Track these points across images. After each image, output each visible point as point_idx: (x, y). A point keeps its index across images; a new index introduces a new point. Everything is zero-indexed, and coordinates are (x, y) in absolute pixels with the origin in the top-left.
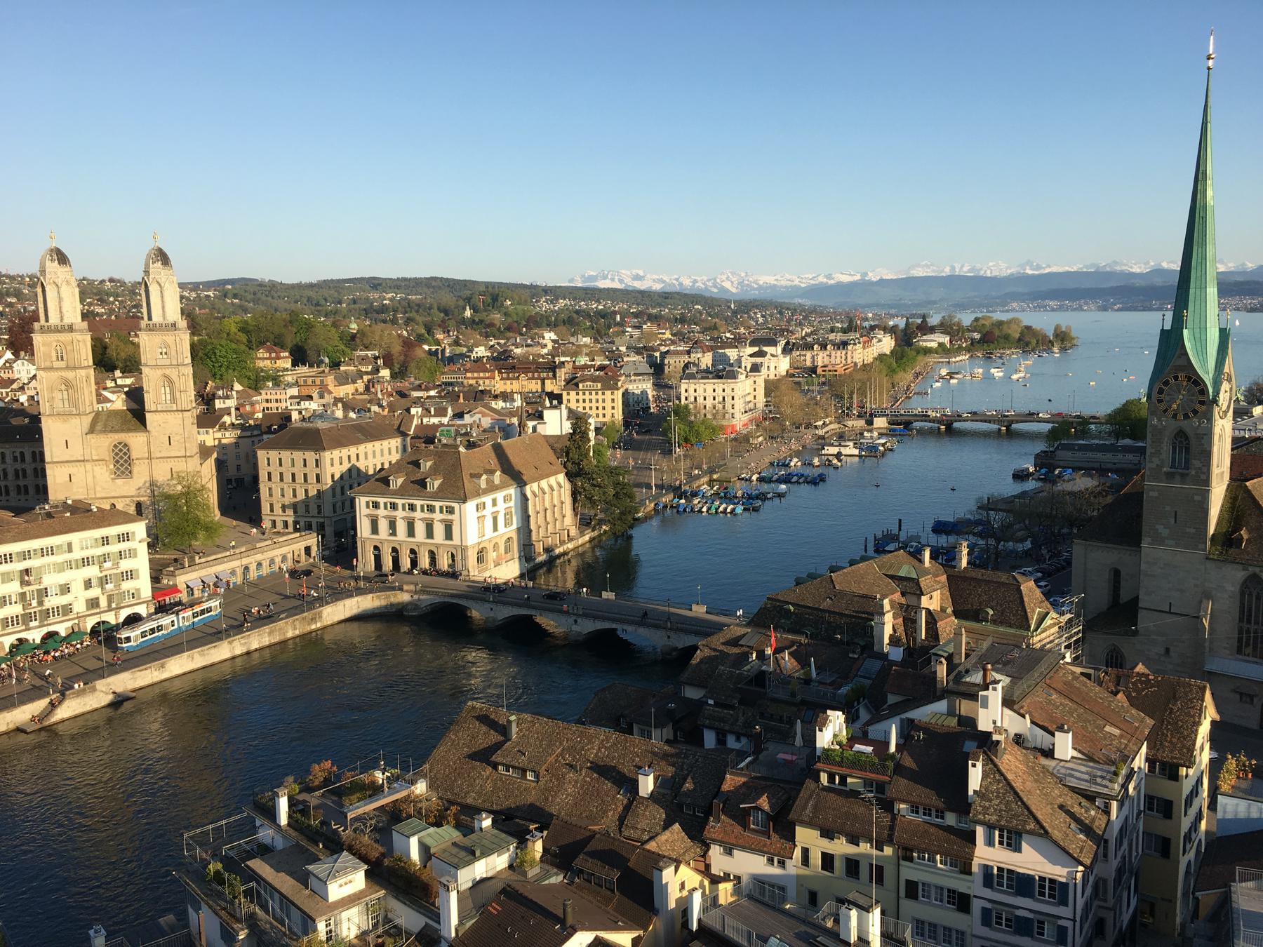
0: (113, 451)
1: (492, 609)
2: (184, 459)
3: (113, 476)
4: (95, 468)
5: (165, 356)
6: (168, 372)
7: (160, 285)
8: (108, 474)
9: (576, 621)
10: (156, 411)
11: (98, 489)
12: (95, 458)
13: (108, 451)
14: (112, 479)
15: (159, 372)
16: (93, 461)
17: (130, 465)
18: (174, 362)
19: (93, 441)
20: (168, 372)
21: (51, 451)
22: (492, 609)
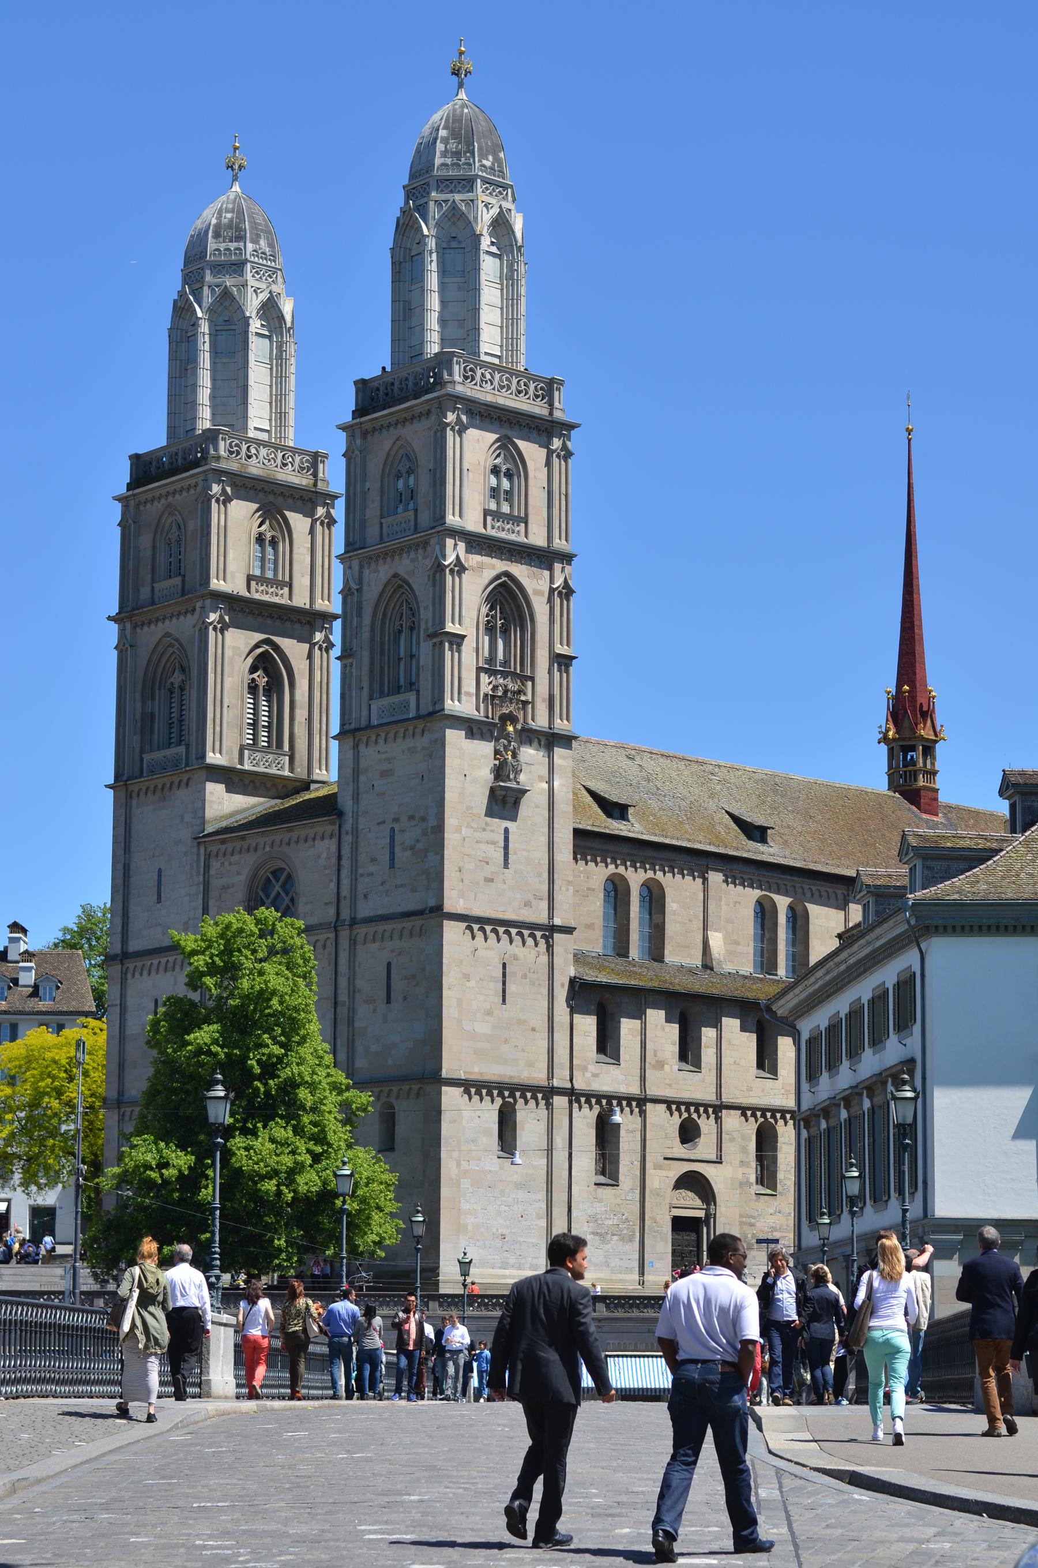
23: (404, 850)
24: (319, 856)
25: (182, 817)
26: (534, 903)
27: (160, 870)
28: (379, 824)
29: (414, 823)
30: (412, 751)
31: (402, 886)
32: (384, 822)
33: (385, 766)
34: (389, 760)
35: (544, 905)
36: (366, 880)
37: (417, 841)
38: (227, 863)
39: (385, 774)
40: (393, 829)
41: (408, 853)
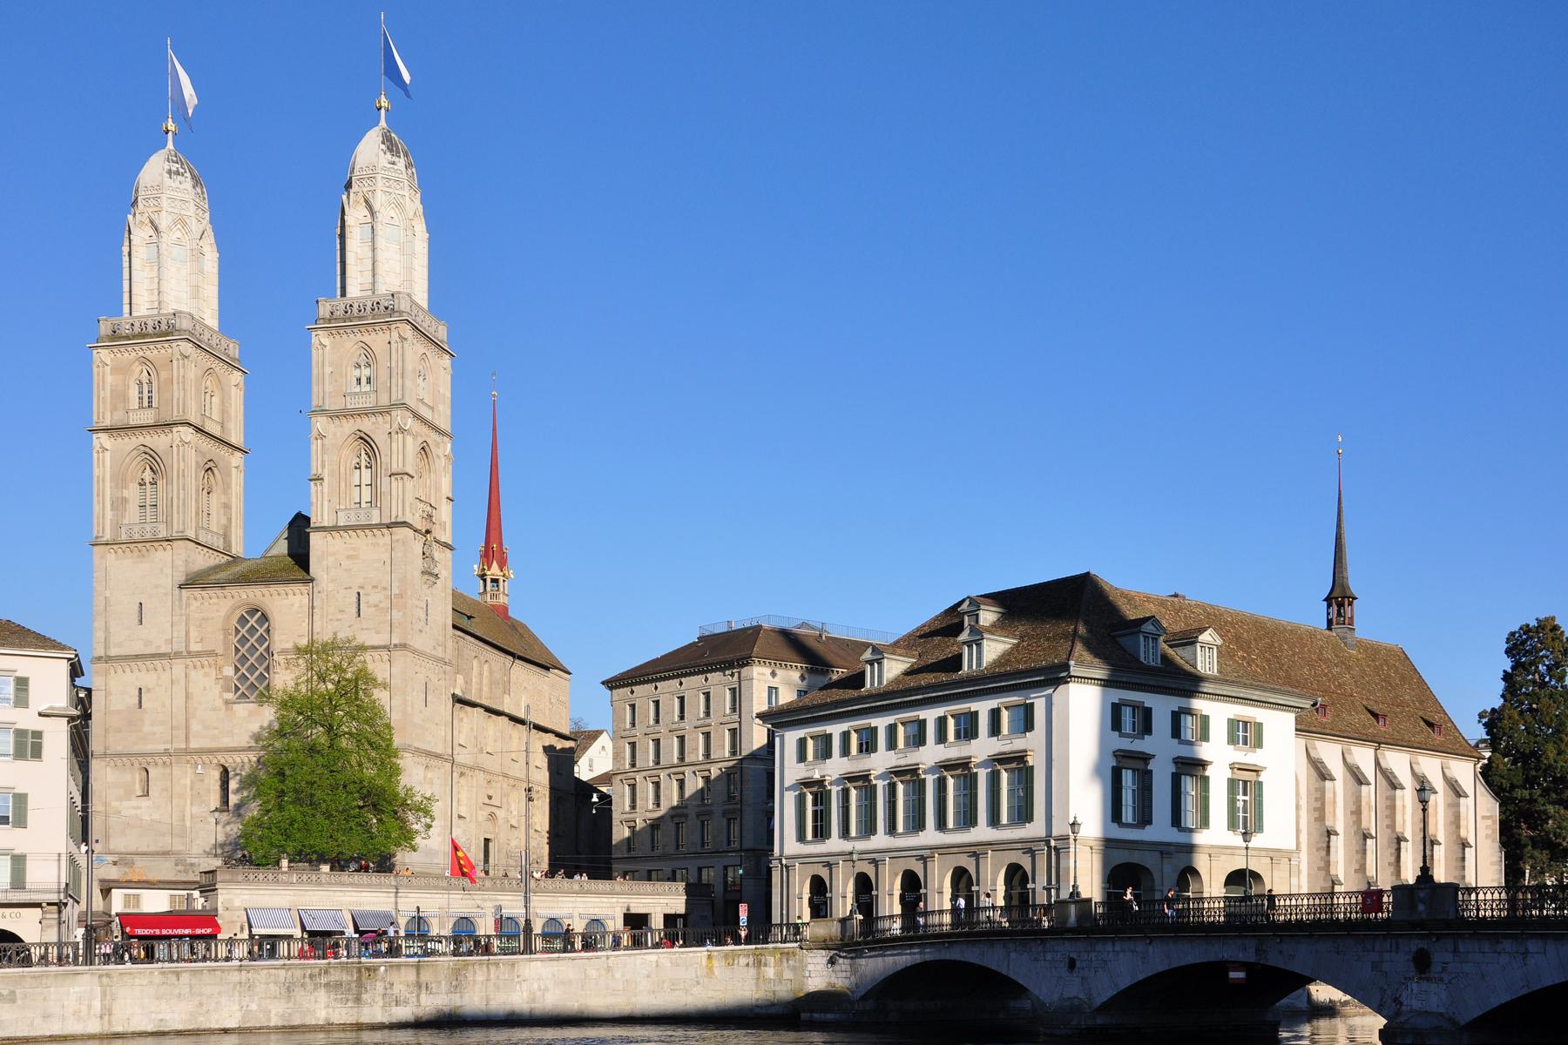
0: (237, 631)
1: (1072, 964)
2: (384, 654)
3: (230, 696)
4: (193, 674)
5: (367, 388)
6: (366, 425)
7: (372, 213)
8: (218, 688)
9: (1422, 963)
10: (336, 528)
11: (195, 727)
12: (194, 647)
13: (226, 631)
14: (227, 702)
15: (349, 426)
16: (190, 654)
17: (267, 669)
18: (384, 401)
19: (195, 604)
20: (366, 425)
21: (107, 629)
22: (1072, 964)
23: (369, 606)
24: (292, 605)
25: (162, 570)
26: (437, 647)
27: (141, 604)
28: (346, 588)
29: (376, 590)
30: (375, 545)
31: (367, 629)
32: (350, 588)
33: (352, 553)
34: (354, 549)
35: (440, 649)
36: (336, 623)
37: (380, 602)
38: (206, 604)
39: (349, 557)
40: (359, 594)
41: (374, 609)
